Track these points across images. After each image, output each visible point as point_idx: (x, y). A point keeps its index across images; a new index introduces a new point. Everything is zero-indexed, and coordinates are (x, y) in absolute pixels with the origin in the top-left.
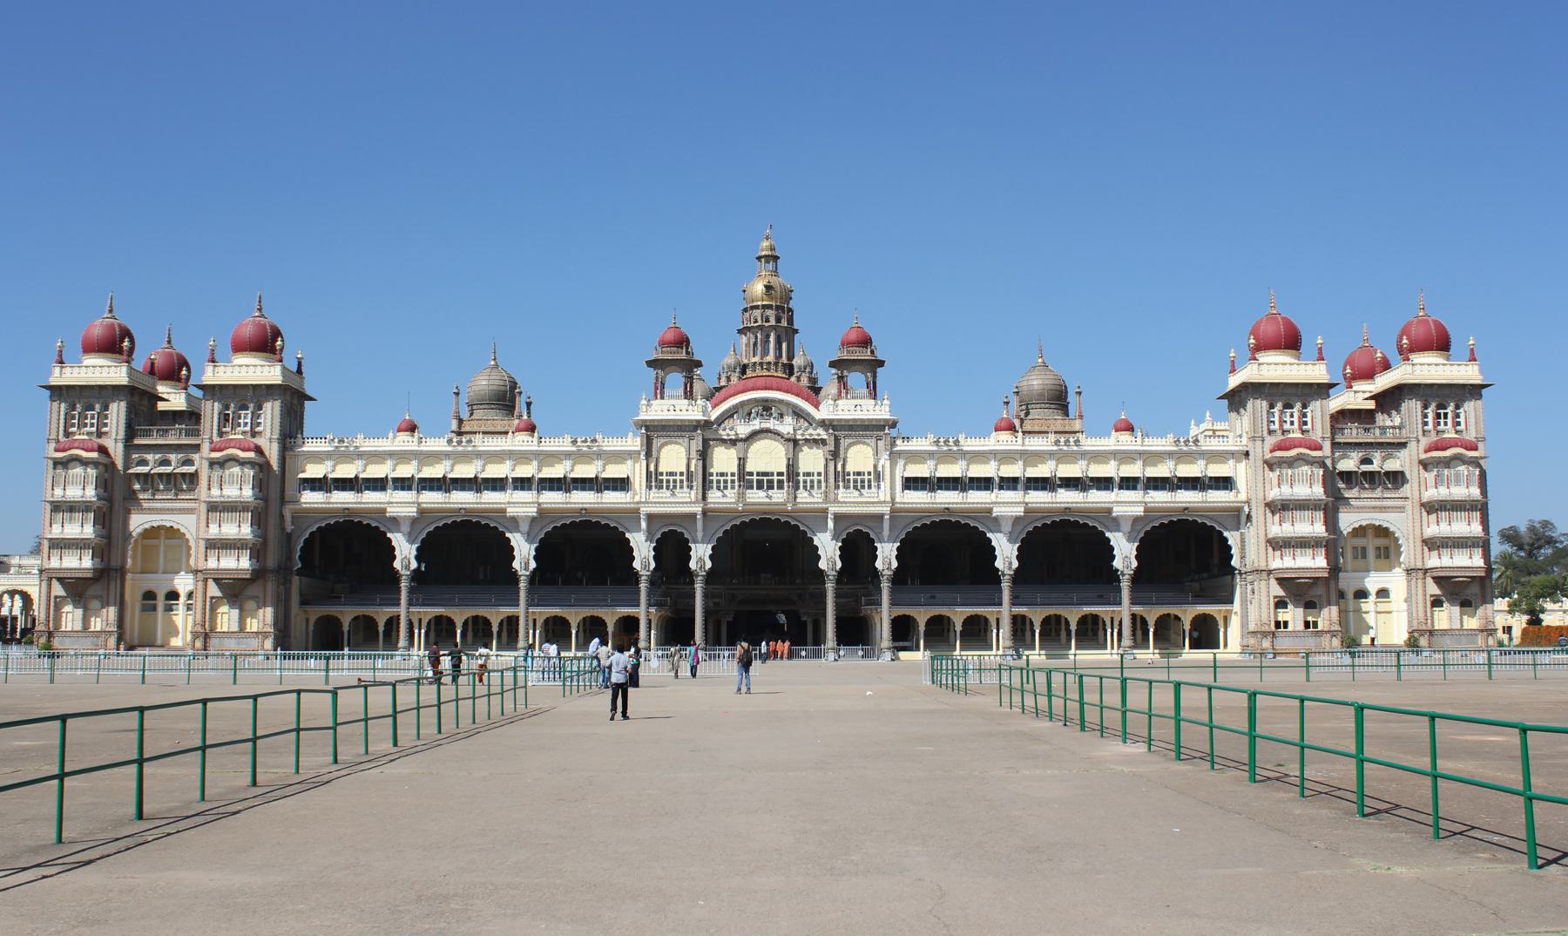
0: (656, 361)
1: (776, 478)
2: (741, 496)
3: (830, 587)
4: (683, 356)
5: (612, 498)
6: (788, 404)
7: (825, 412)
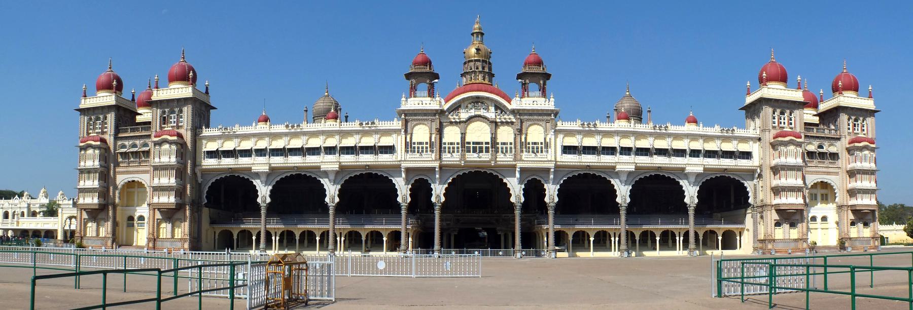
0: (411, 73)
1: (484, 146)
2: (463, 156)
3: (517, 213)
4: (428, 70)
5: (384, 159)
6: (492, 100)
7: (516, 104)
